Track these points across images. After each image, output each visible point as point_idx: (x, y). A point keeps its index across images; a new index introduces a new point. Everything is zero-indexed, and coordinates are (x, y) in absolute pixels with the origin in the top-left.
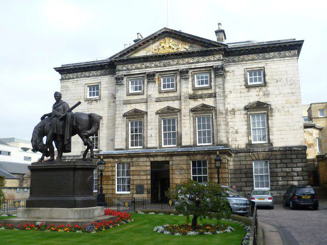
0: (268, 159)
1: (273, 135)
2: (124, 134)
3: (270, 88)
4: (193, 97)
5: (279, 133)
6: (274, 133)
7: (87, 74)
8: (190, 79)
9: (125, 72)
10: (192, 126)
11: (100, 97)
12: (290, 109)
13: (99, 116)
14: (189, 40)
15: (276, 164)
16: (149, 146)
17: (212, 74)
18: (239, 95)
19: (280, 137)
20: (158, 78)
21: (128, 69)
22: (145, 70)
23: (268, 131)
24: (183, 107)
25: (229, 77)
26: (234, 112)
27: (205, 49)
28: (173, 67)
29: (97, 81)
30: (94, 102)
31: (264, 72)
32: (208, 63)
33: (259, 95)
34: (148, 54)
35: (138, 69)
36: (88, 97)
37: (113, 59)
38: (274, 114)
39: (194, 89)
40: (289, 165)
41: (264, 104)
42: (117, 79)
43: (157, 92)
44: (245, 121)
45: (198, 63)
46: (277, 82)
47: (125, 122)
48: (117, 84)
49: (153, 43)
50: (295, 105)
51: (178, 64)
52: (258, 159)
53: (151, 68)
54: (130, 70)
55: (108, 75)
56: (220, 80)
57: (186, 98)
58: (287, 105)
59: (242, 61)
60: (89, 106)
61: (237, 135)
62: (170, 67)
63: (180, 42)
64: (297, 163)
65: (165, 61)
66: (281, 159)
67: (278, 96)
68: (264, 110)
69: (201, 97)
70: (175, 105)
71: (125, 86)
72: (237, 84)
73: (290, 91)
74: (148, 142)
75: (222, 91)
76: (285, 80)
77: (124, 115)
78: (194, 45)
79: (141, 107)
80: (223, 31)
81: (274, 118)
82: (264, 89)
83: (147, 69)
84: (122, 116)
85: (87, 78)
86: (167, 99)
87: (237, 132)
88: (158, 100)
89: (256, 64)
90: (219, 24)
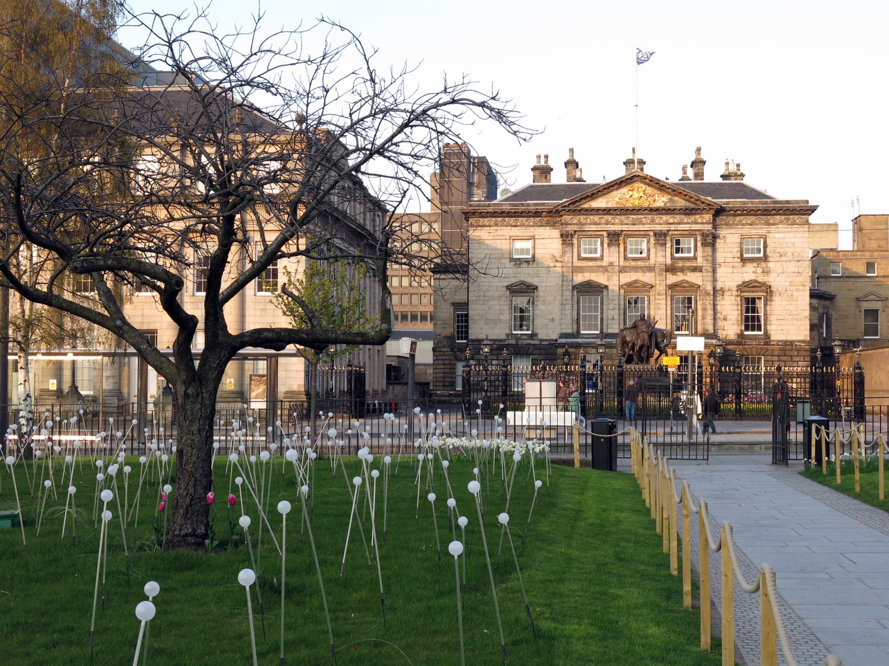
0: (763, 355)
1: (771, 325)
2: (575, 313)
3: (771, 265)
4: (671, 269)
5: (778, 322)
6: (773, 322)
7: (512, 220)
8: (669, 245)
9: (576, 226)
10: (669, 308)
11: (534, 257)
12: (796, 294)
13: (534, 286)
14: (670, 190)
15: (773, 361)
16: (610, 331)
17: (699, 238)
18: (730, 270)
19: (780, 328)
20: (624, 239)
21: (580, 224)
22: (606, 226)
23: (766, 320)
24: (658, 282)
25: (719, 243)
26: (723, 292)
27: (692, 206)
28: (646, 226)
29: (530, 234)
30: (525, 265)
31: (765, 243)
32: (693, 226)
33: (756, 272)
34: (610, 205)
35: (595, 224)
36: (515, 257)
37: (560, 208)
38: (774, 298)
39: (673, 258)
40: (788, 364)
41: (764, 284)
42: (562, 235)
43: (622, 259)
44: (738, 305)
45: (679, 224)
46: (781, 256)
47: (576, 298)
48: (564, 243)
49: (616, 190)
50: (801, 288)
51: (653, 222)
52: (750, 353)
53: (616, 225)
54: (584, 225)
55: (546, 226)
56: (709, 249)
57: (662, 270)
58: (792, 288)
59: (737, 225)
60: (516, 270)
61: (725, 323)
62: (640, 226)
63: (656, 191)
64: (798, 362)
65: (634, 217)
66: (778, 356)
67: (781, 275)
68: (762, 291)
69: (682, 270)
70: (647, 278)
71: (576, 246)
72: (729, 255)
73: (796, 270)
74: (609, 326)
75: (710, 265)
76: (790, 254)
77: (574, 287)
78: (676, 198)
79: (600, 278)
80: (704, 163)
81: (773, 303)
82: (763, 264)
83: (608, 226)
84: (571, 288)
85: (513, 228)
86: (636, 269)
87: (725, 319)
88: (622, 270)
89: (755, 229)
90: (699, 150)
